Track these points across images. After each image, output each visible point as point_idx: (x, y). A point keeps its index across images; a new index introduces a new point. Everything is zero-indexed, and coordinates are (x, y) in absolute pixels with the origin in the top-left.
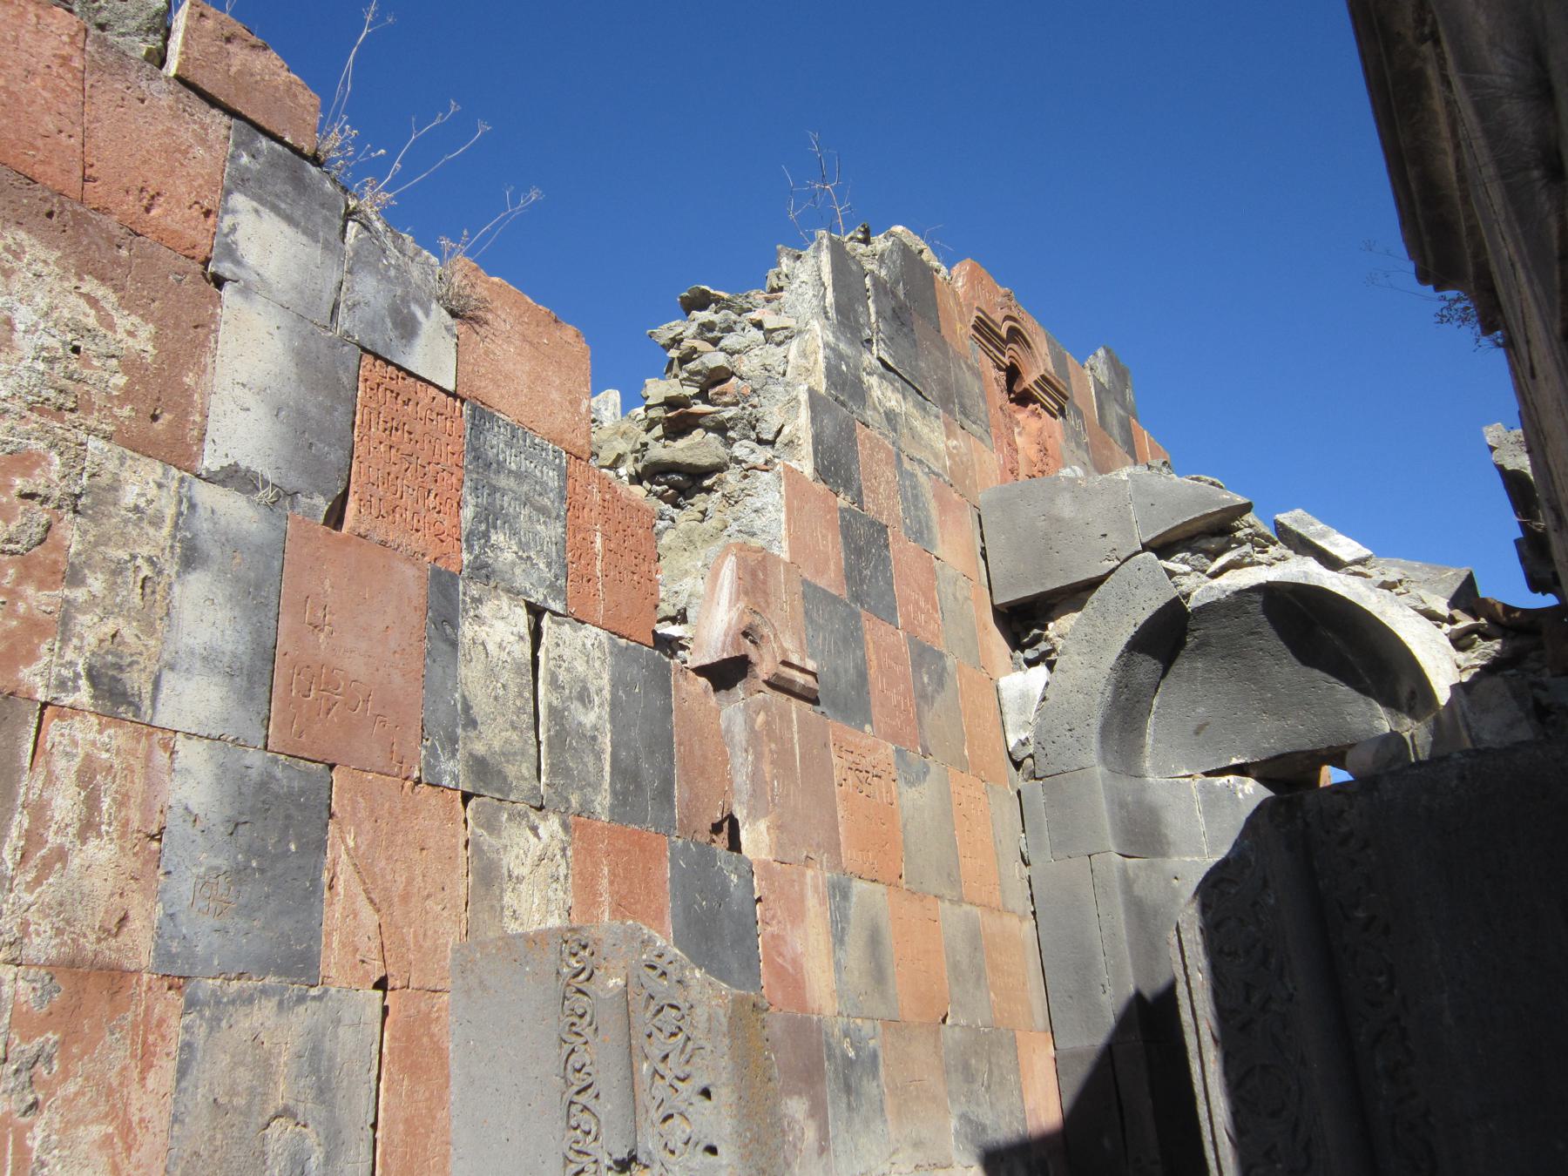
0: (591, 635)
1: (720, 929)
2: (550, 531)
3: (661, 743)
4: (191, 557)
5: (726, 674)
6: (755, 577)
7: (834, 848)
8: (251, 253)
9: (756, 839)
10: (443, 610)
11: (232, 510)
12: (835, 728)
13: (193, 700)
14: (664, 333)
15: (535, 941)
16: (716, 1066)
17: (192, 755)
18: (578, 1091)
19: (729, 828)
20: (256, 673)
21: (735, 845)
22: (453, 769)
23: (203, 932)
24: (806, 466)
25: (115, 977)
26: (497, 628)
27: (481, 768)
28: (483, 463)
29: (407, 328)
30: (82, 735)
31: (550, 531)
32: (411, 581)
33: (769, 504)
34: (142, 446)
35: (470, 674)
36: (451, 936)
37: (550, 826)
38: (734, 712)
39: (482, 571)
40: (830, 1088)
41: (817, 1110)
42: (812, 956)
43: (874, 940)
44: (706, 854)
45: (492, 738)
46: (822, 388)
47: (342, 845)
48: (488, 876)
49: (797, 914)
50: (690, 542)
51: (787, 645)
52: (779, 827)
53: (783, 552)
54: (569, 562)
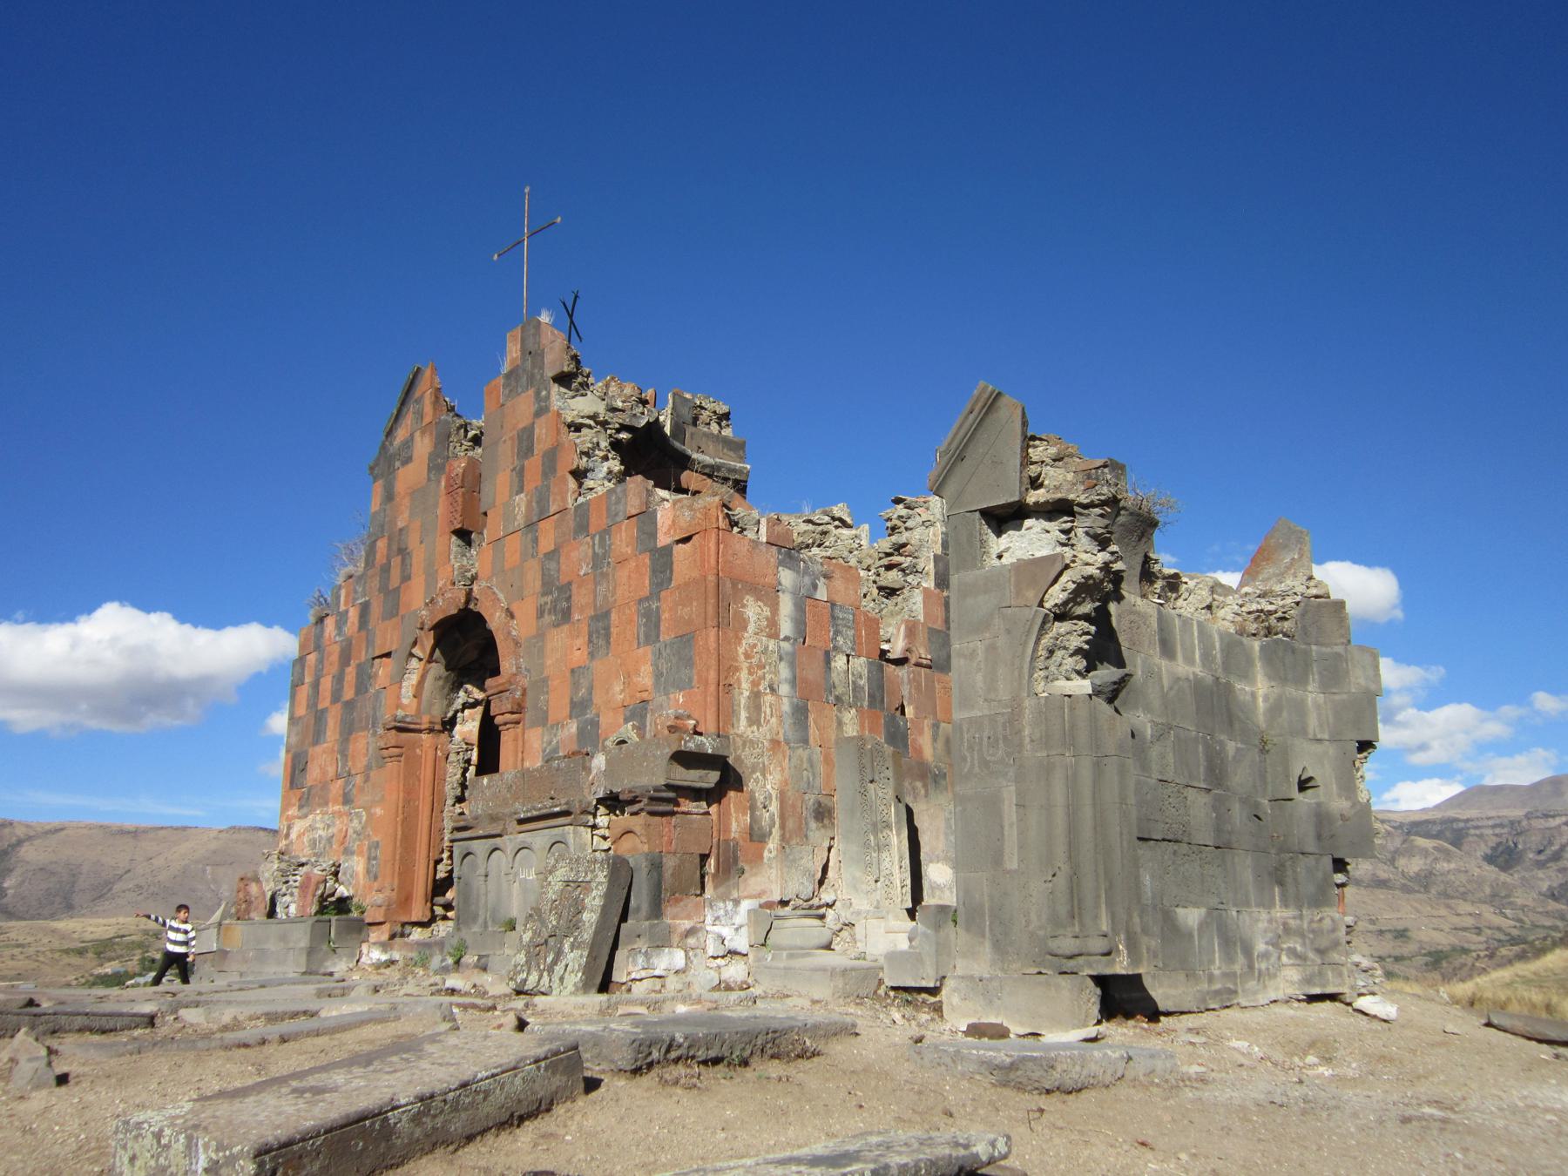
0: (863, 659)
1: (898, 737)
2: (851, 633)
3: (881, 687)
4: (781, 659)
5: (901, 662)
6: (911, 632)
7: (935, 713)
8: (783, 581)
9: (910, 711)
10: (828, 660)
11: (786, 646)
12: (937, 675)
13: (784, 689)
14: (886, 513)
15: (853, 738)
16: (889, 763)
17: (785, 700)
18: (862, 768)
19: (902, 709)
20: (793, 682)
21: (903, 713)
22: (831, 698)
23: (790, 735)
24: (929, 583)
25: (778, 742)
26: (839, 662)
27: (838, 698)
28: (834, 617)
29: (815, 587)
30: (769, 698)
31: (851, 633)
32: (820, 654)
33: (915, 603)
34: (770, 636)
35: (834, 675)
36: (833, 738)
37: (853, 711)
38: (902, 672)
39: (835, 648)
40: (929, 781)
41: (925, 786)
42: (926, 746)
43: (948, 741)
44: (893, 716)
45: (839, 691)
46: (939, 552)
47: (811, 717)
48: (840, 723)
49: (921, 732)
50: (892, 614)
51: (922, 652)
52: (916, 708)
53: (921, 618)
54: (856, 641)
